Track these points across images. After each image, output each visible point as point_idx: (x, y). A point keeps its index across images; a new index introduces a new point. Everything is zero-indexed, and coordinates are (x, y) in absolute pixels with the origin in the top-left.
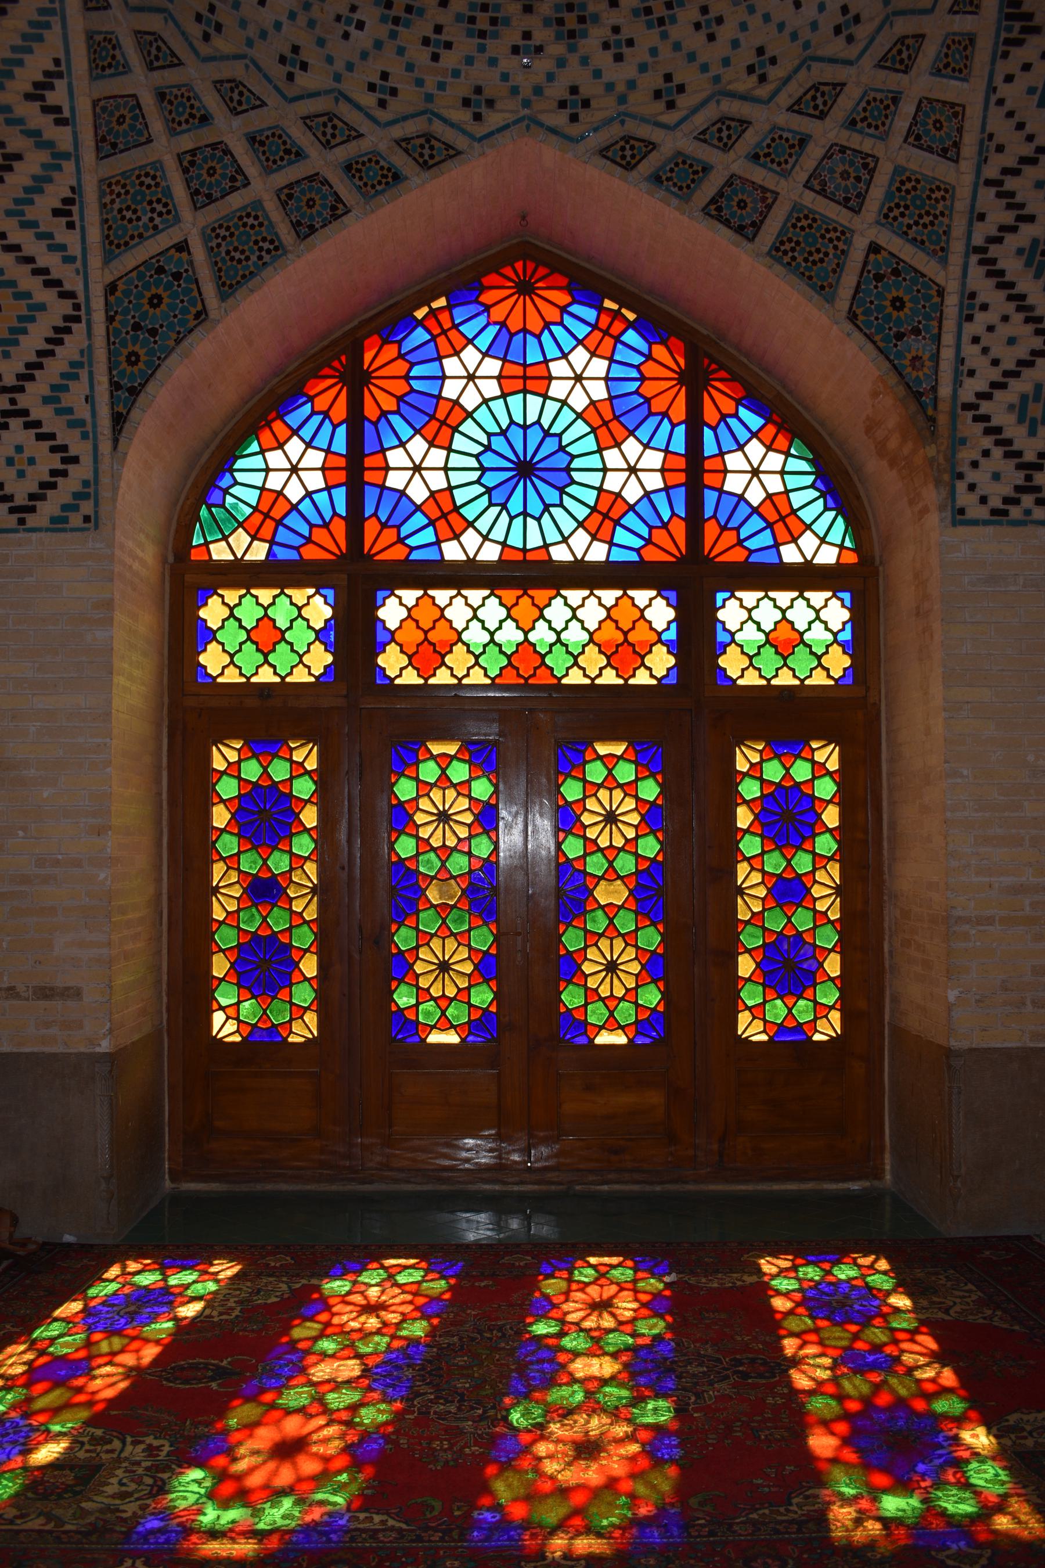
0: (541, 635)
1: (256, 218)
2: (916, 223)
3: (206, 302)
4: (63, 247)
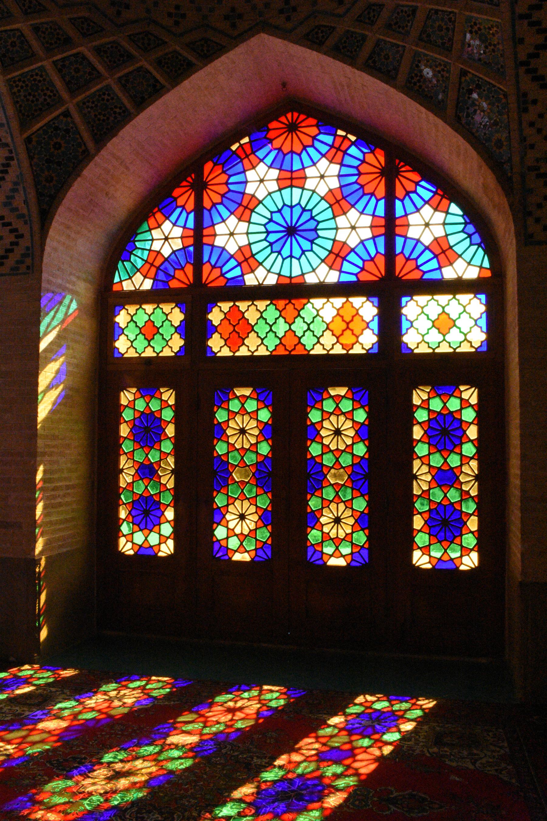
0: (299, 327)
1: (109, 95)
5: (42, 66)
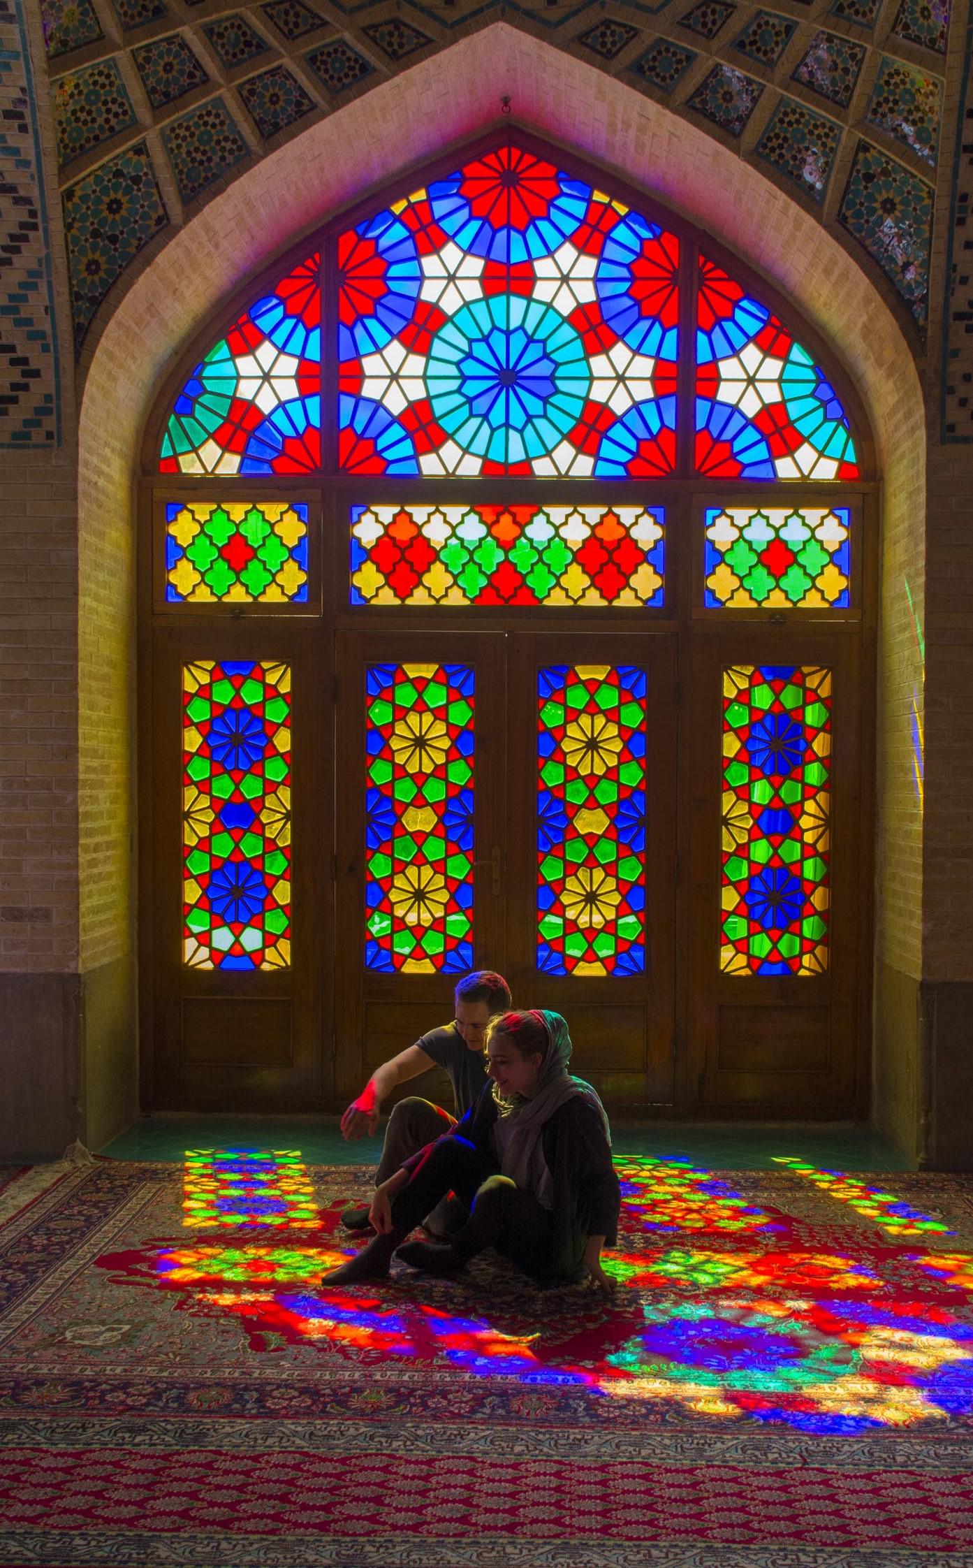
0: (522, 557)
1: (217, 116)
4: (16, 151)
5: (113, 59)
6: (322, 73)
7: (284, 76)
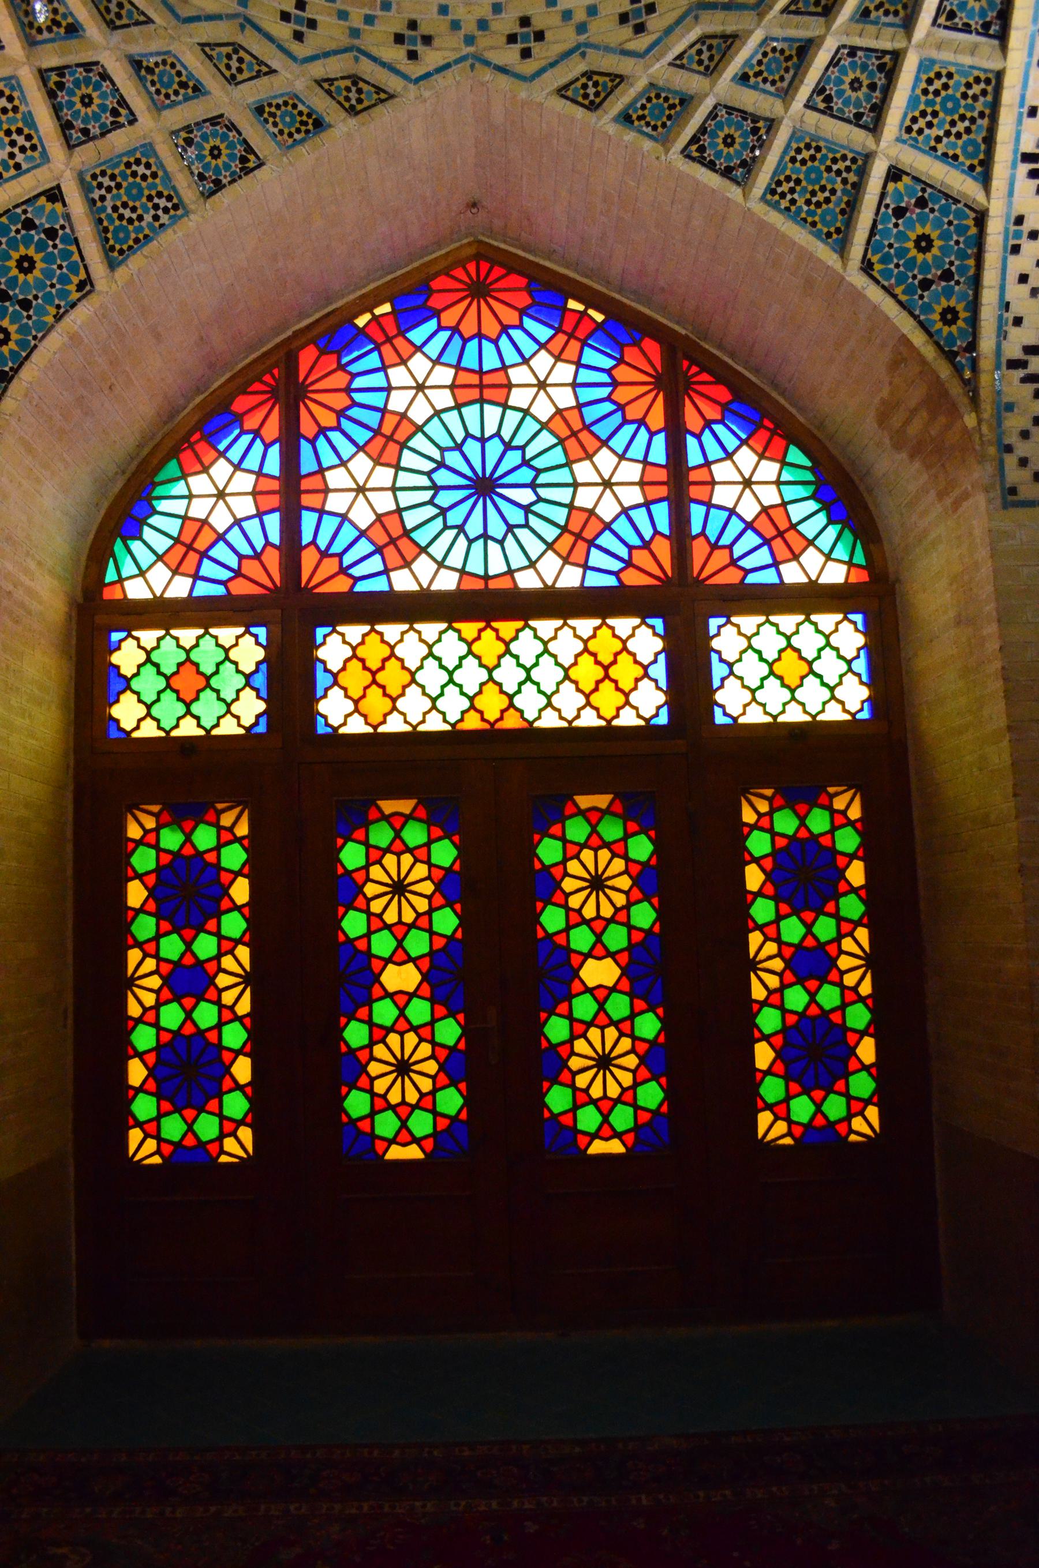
1: (148, 166)
2: (948, 134)
3: (91, 270)
6: (270, 126)
7: (226, 126)
